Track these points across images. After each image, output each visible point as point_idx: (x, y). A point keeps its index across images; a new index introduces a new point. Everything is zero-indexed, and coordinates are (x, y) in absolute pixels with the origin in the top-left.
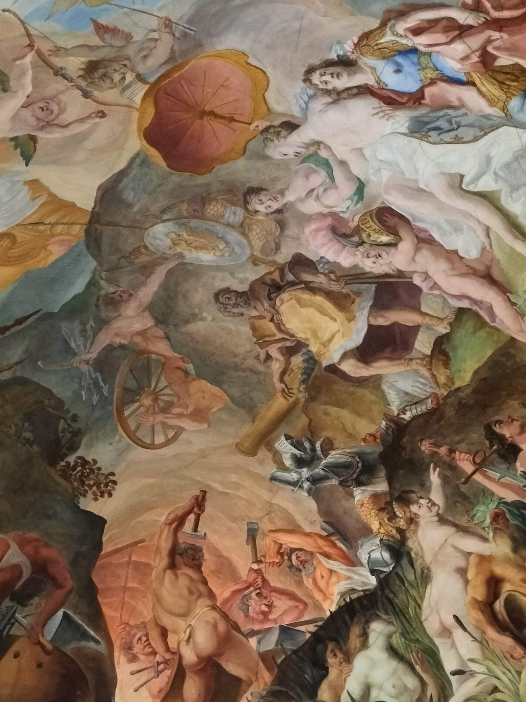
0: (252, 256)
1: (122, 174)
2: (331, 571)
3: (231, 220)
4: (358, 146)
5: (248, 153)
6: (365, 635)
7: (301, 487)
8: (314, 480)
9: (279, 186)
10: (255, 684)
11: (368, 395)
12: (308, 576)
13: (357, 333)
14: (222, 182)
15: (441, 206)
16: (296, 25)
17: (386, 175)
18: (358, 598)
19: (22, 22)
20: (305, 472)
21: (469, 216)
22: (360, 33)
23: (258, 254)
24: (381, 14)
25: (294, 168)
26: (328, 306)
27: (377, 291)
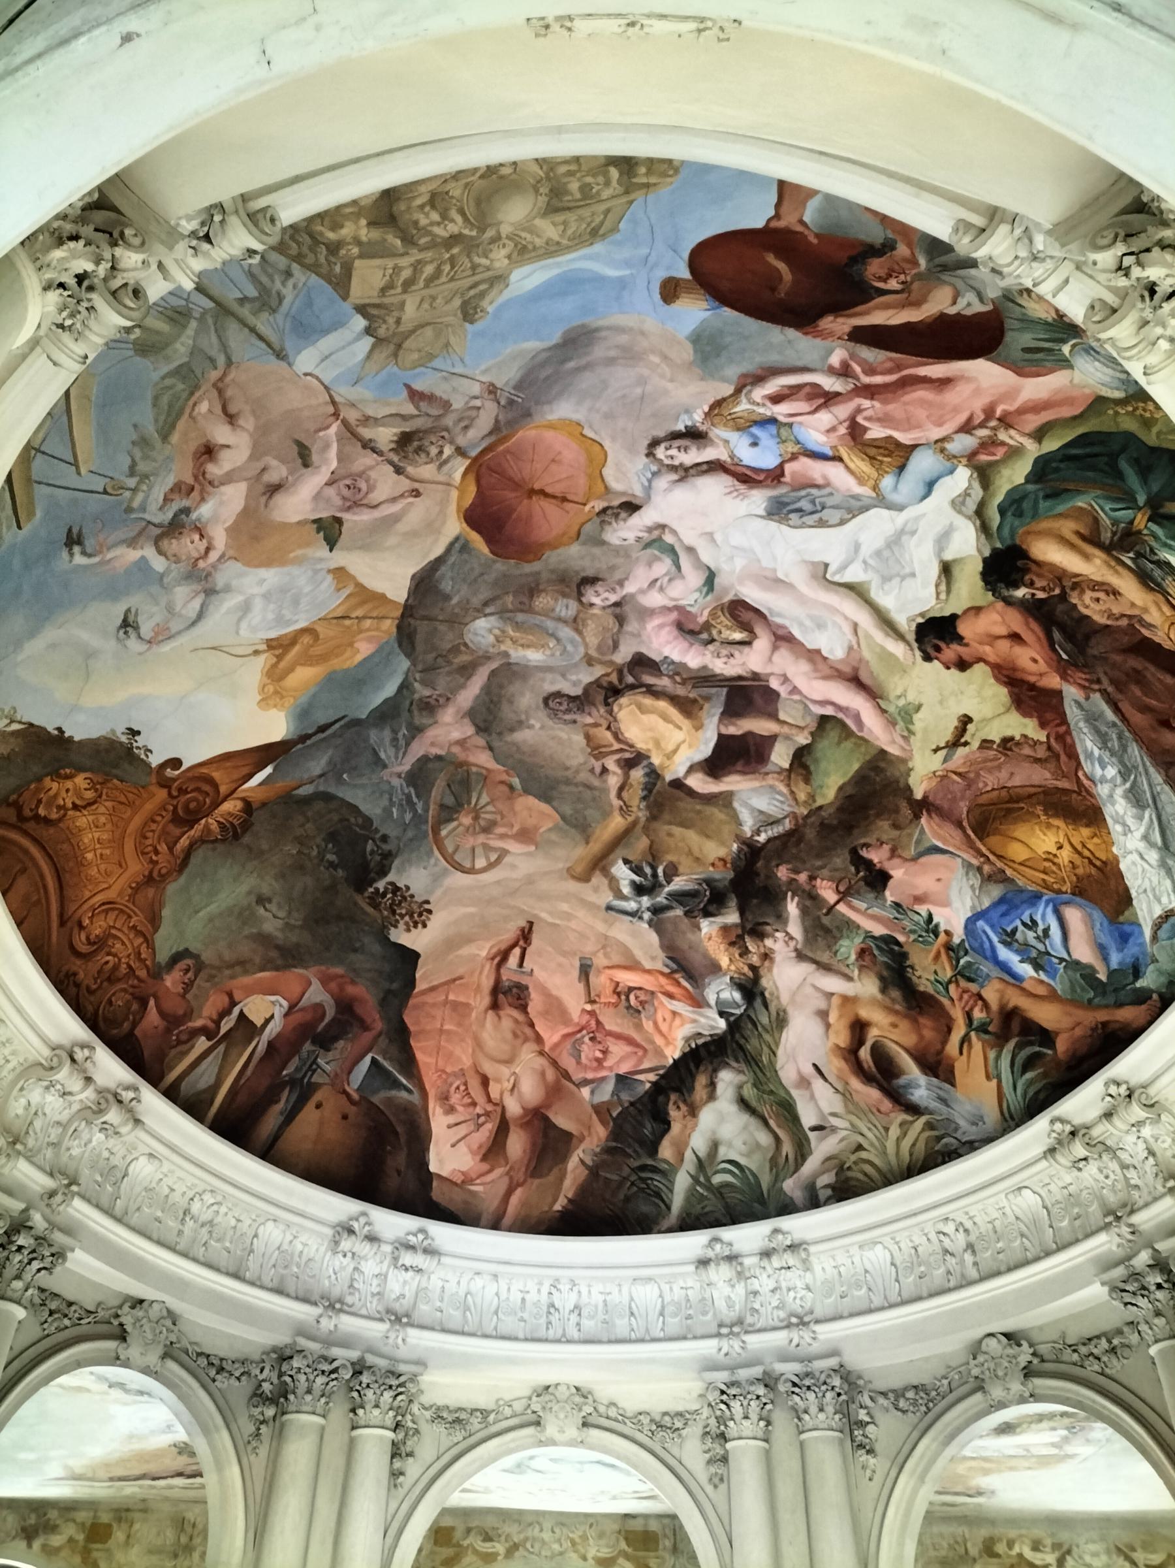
0: (586, 654)
1: (439, 561)
2: (674, 1013)
3: (563, 614)
4: (708, 530)
5: (582, 537)
6: (712, 1085)
7: (641, 918)
8: (656, 910)
9: (618, 575)
10: (588, 1139)
11: (718, 814)
12: (648, 1018)
13: (706, 743)
14: (552, 571)
15: (802, 600)
16: (639, 391)
17: (739, 563)
18: (705, 1044)
19: (326, 388)
20: (646, 901)
21: (835, 611)
22: (712, 401)
23: (593, 653)
24: (735, 379)
25: (634, 555)
26: (673, 712)
27: (728, 694)
